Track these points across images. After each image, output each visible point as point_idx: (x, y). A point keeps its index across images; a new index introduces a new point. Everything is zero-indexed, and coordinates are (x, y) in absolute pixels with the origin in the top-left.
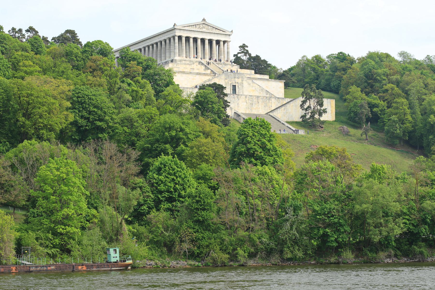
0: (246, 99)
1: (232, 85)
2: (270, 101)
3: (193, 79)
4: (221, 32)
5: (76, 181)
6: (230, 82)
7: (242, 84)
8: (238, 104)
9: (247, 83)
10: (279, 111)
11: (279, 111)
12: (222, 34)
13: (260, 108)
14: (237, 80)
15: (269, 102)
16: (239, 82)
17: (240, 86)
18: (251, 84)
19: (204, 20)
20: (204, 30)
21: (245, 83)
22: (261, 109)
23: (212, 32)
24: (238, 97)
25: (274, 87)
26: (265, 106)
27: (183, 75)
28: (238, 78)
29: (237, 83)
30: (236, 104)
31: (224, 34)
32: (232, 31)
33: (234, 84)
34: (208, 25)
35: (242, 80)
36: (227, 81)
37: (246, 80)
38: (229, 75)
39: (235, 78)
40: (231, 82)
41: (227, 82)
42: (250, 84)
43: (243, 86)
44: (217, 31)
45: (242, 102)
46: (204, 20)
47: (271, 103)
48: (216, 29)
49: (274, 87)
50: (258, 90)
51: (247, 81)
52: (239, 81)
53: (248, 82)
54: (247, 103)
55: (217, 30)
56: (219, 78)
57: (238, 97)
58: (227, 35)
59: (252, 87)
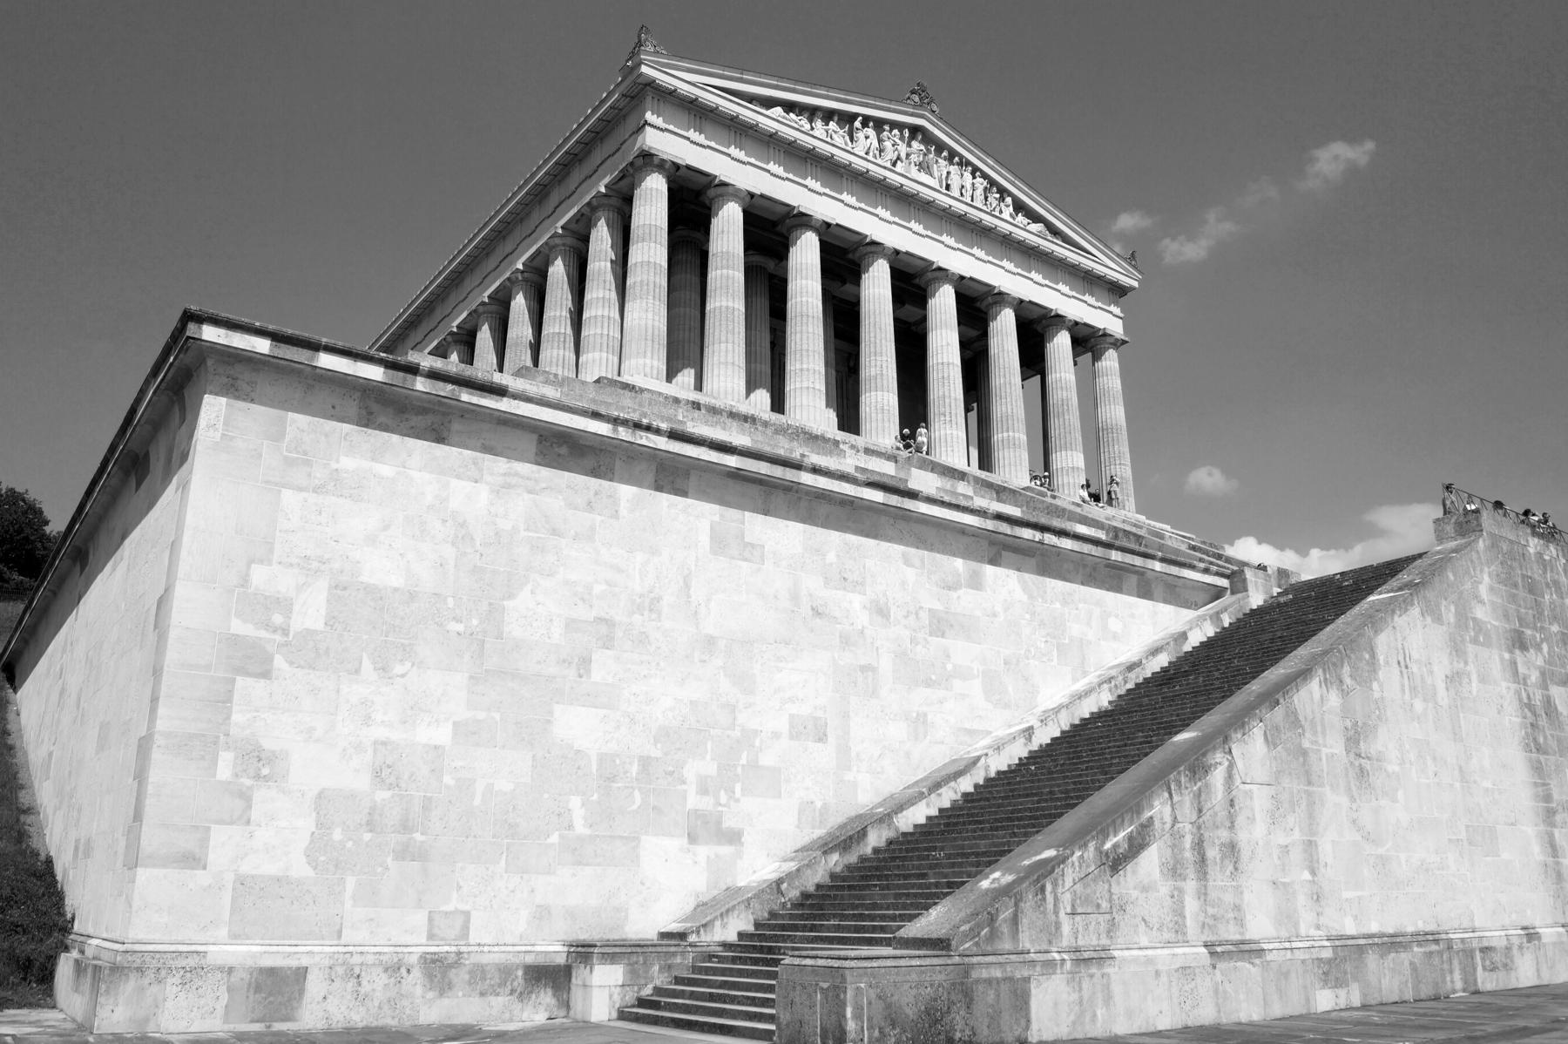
3: (940, 625)
34: (961, 157)
48: (1019, 207)
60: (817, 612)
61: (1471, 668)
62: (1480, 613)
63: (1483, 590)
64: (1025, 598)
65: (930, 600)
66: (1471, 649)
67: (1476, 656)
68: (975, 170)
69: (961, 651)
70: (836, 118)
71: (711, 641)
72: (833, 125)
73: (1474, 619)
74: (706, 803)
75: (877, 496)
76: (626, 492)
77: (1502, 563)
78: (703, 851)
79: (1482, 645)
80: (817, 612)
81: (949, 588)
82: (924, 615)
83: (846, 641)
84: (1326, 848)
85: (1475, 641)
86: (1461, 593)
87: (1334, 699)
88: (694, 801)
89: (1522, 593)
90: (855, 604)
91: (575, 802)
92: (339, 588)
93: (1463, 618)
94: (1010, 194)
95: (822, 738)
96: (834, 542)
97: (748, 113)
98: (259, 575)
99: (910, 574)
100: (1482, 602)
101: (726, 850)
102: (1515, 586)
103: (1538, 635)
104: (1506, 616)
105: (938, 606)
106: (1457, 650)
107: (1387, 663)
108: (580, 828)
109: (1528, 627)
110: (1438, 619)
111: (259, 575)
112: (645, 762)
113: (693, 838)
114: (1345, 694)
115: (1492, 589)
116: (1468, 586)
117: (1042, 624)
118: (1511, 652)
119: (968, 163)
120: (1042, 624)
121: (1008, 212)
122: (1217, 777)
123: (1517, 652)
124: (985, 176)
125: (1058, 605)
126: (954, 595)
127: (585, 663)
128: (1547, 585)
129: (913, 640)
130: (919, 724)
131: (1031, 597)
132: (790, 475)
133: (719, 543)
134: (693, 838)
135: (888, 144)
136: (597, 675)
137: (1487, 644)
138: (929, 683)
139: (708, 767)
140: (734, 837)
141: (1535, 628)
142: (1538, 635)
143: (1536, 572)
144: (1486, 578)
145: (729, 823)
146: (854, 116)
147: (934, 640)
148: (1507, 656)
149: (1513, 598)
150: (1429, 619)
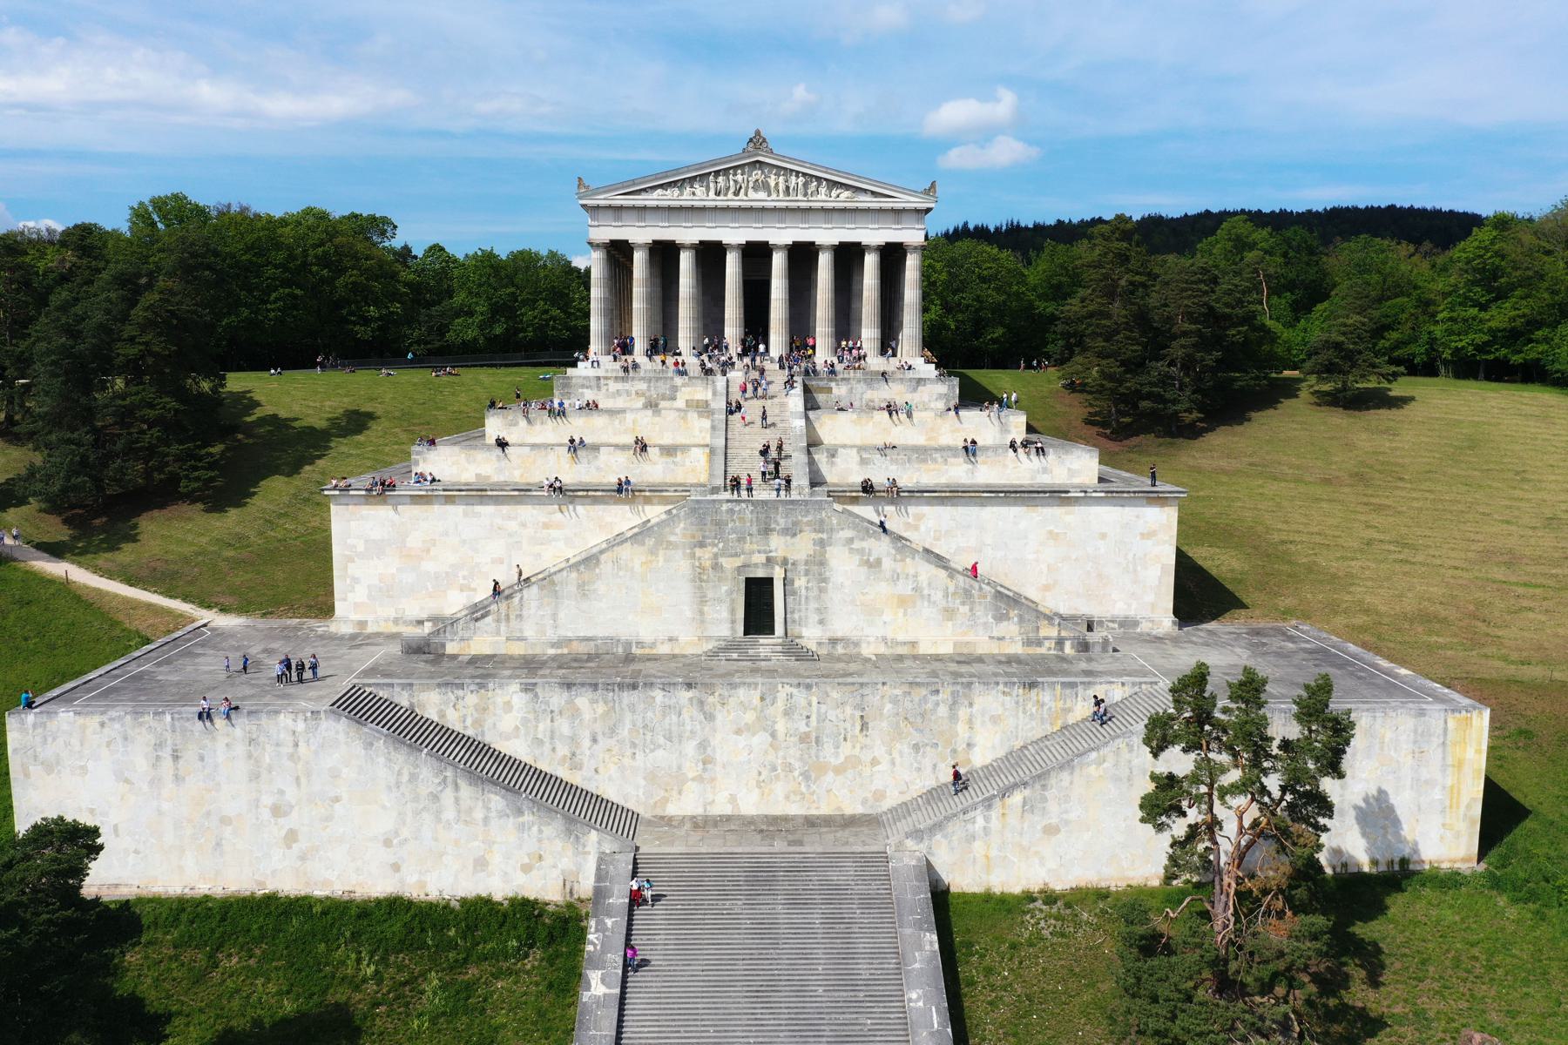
0: (771, 711)
1: (742, 578)
2: (963, 713)
3: (546, 526)
4: (865, 201)
5: (1143, 379)
6: (729, 564)
7: (822, 563)
8: (703, 745)
9: (857, 558)
10: (980, 821)
11: (980, 821)
12: (868, 210)
13: (875, 762)
14: (778, 545)
15: (953, 717)
16: (792, 557)
17: (800, 583)
18: (887, 564)
19: (757, 141)
20: (758, 198)
21: (842, 563)
22: (884, 766)
23: (803, 205)
24: (701, 703)
25: (1103, 536)
26: (916, 747)
27: (478, 508)
28: (791, 531)
29: (785, 562)
30: (690, 748)
31: (881, 210)
32: (931, 190)
33: (760, 573)
34: (785, 169)
35: (822, 544)
36: (706, 555)
37: (851, 540)
38: (725, 517)
39: (766, 531)
40: (738, 562)
41: (708, 564)
42: (878, 562)
43: (825, 580)
44: (843, 198)
45: (738, 732)
46: (757, 141)
47: (970, 722)
48: (833, 184)
49: (1103, 536)
50: (938, 596)
51: (857, 545)
52: (800, 548)
53: (861, 551)
54: (773, 735)
55: (834, 193)
56: (650, 542)
57: (701, 703)
58: (904, 210)
59: (895, 578)
60: (499, 528)
65: (543, 519)
68: (798, 173)
69: (554, 533)
71: (464, 542)
72: (696, 185)
74: (466, 582)
75: (516, 493)
76: (436, 507)
78: (465, 594)
80: (499, 528)
83: (510, 535)
84: (561, 615)
88: (462, 582)
90: (512, 525)
92: (366, 541)
94: (826, 179)
95: (502, 563)
96: (505, 509)
97: (638, 201)
98: (348, 541)
99: (535, 512)
101: (472, 593)
105: (547, 520)
108: (431, 590)
111: (348, 541)
112: (447, 573)
113: (462, 590)
119: (792, 171)
121: (823, 190)
124: (804, 175)
127: (428, 551)
129: (535, 532)
130: (539, 555)
132: (483, 493)
133: (466, 514)
134: (462, 590)
135: (732, 182)
136: (432, 553)
138: (542, 544)
139: (466, 573)
140: (475, 590)
145: (472, 586)
146: (710, 173)
147: (544, 531)
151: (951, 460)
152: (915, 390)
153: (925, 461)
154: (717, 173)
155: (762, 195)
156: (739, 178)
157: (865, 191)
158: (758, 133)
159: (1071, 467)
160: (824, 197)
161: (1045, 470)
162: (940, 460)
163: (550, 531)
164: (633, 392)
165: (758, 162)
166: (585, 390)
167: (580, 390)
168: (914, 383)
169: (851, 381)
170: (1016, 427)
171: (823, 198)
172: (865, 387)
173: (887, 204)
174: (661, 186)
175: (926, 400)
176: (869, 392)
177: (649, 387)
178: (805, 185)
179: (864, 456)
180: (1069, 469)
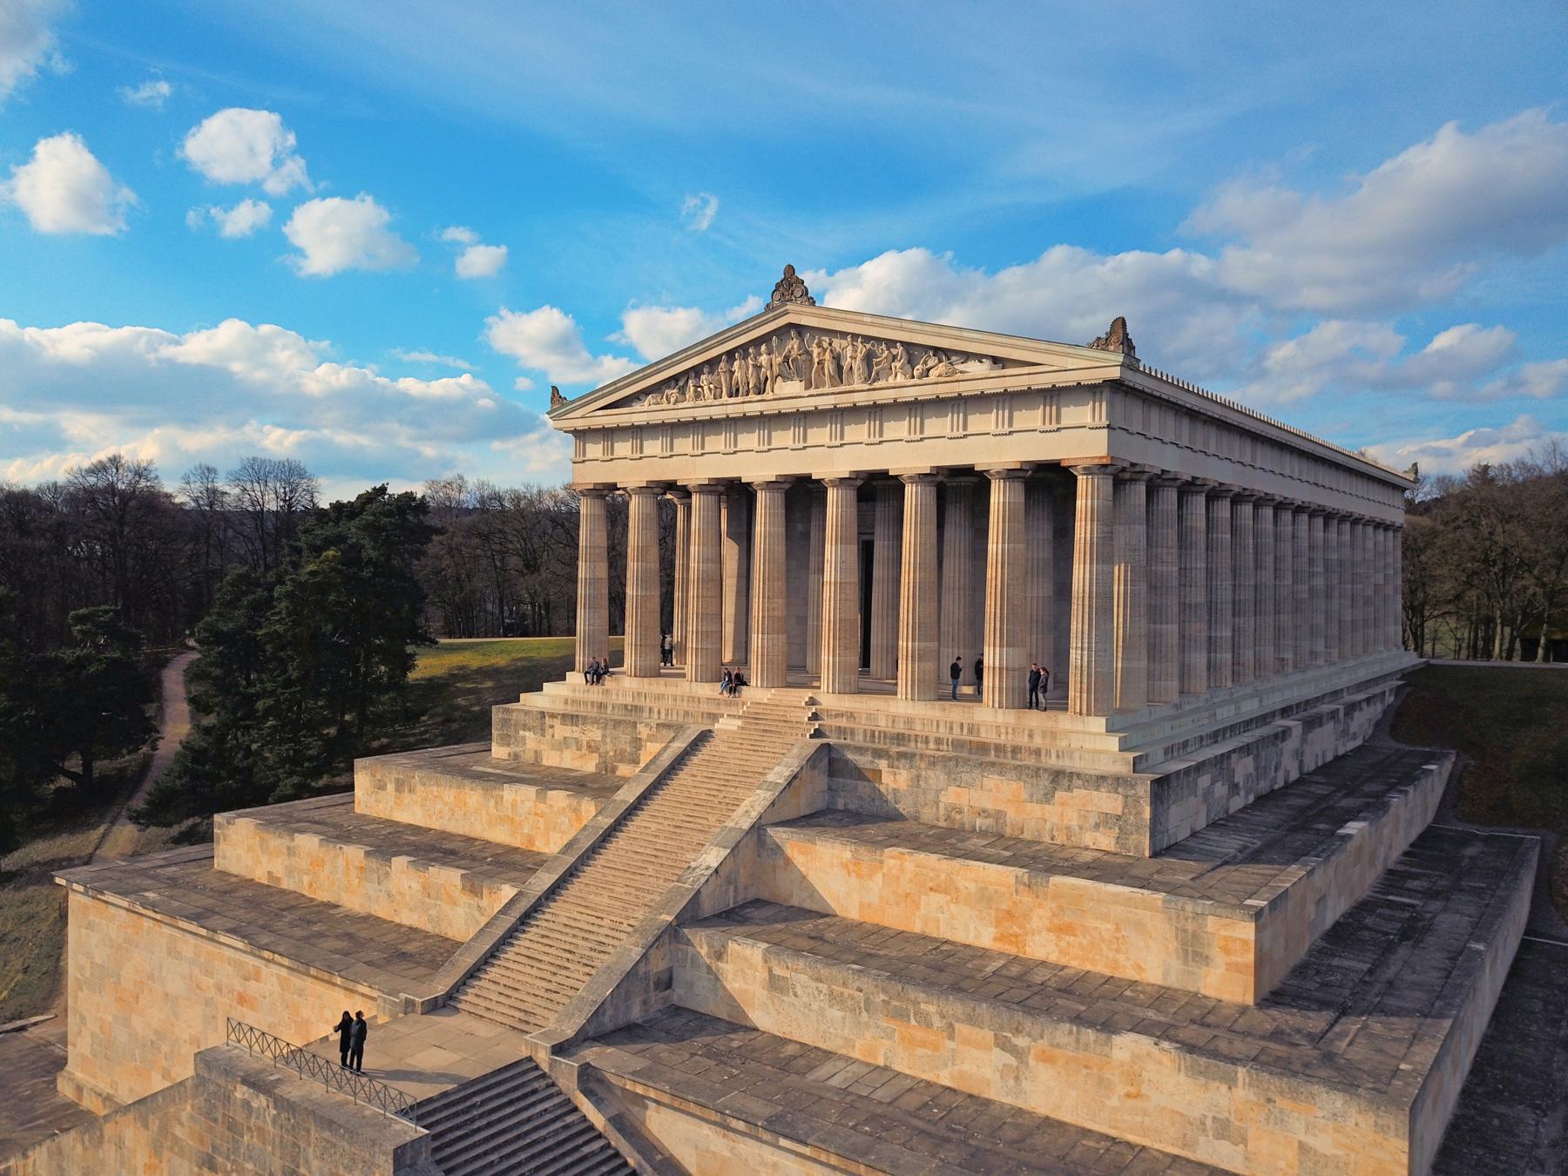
4: (977, 377)
20: (790, 393)
61: (164, 1165)
62: (179, 1131)
63: (184, 1116)
64: (279, 989)
66: (166, 1154)
67: (169, 1160)
70: (705, 370)
73: (173, 1135)
77: (205, 1100)
79: (177, 1154)
81: (246, 980)
82: (235, 993)
85: (171, 1149)
86: (166, 1114)
87: (79, 1147)
89: (220, 1128)
91: (137, 1051)
93: (164, 1130)
100: (182, 1124)
102: (215, 1120)
103: (229, 1165)
104: (201, 1141)
106: (156, 1150)
107: (109, 1141)
109: (220, 1154)
110: (146, 1127)
112: (152, 1042)
114: (85, 1149)
115: (192, 1117)
116: (172, 1109)
117: (287, 1007)
118: (200, 1168)
120: (287, 1007)
122: (30, 1161)
123: (205, 1170)
124: (866, 339)
125: (296, 996)
126: (247, 983)
128: (249, 1129)
131: (283, 989)
134: (164, 1077)
137: (181, 1154)
141: (228, 1158)
142: (229, 1165)
143: (240, 1117)
144: (189, 1108)
148: (196, 1169)
149: (210, 1130)
150: (139, 1124)
151: (962, 1029)
152: (1048, 798)
153: (900, 1015)
154: (730, 354)
155: (794, 387)
156: (764, 359)
157: (979, 357)
158: (790, 270)
159: (1310, 1140)
160: (900, 379)
161: (1223, 1129)
162: (937, 1022)
163: (244, 1009)
164: (585, 743)
165: (791, 326)
166: (527, 734)
167: (521, 733)
168: (1045, 781)
169: (917, 762)
170: (1227, 951)
171: (899, 385)
172: (942, 777)
173: (1016, 380)
174: (646, 392)
175: (1074, 823)
176: (952, 789)
177: (604, 736)
178: (869, 358)
179: (778, 971)
180: (1303, 1148)
